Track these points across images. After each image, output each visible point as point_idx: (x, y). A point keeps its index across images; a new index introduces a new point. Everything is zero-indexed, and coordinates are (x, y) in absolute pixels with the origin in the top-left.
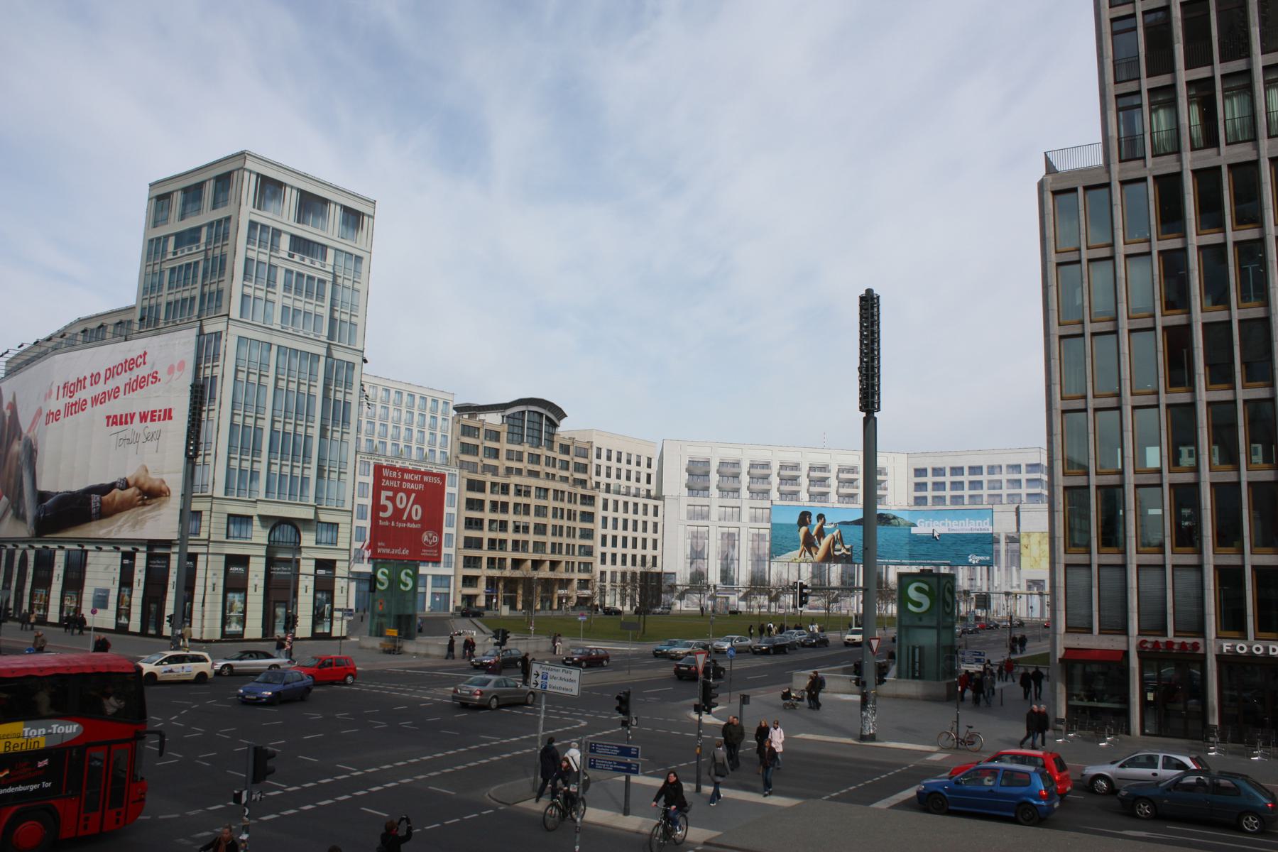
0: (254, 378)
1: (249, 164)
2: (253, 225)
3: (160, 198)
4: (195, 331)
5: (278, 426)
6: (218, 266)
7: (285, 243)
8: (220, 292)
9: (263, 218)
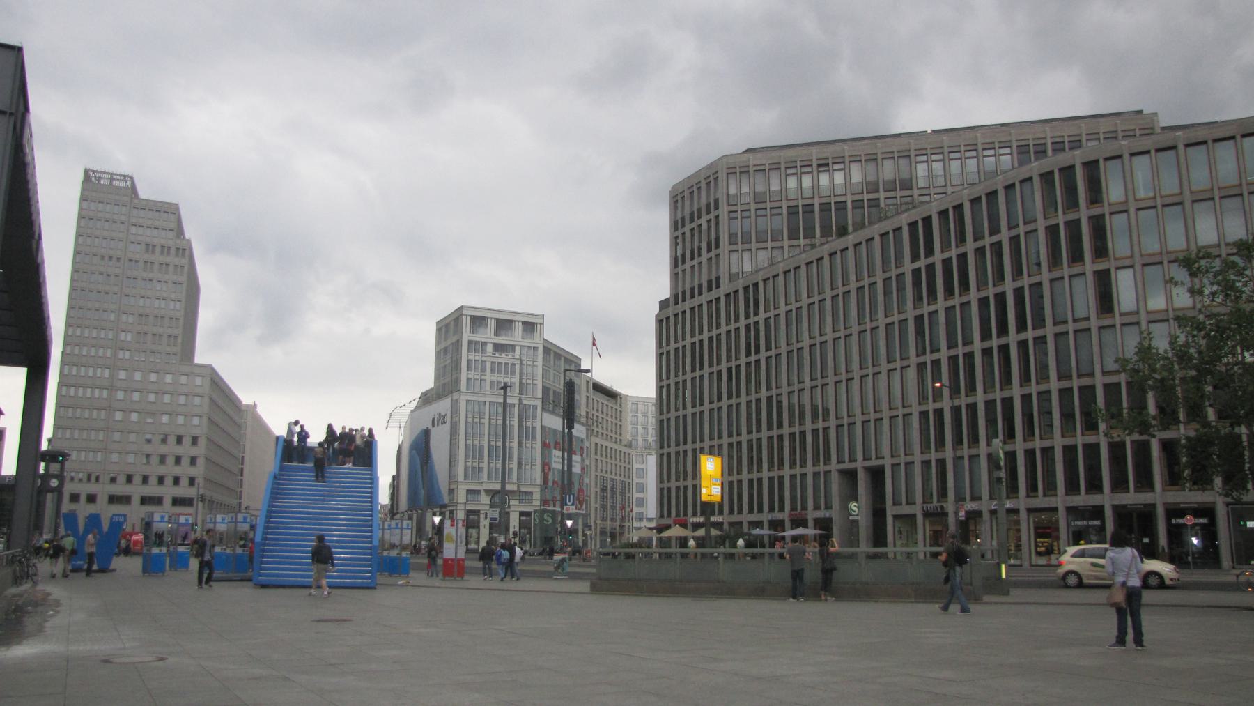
0: (477, 420)
5: (493, 443)
7: (489, 348)
9: (474, 338)
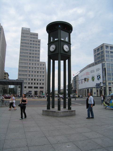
1: (104, 45)
2: (106, 51)
3: (95, 51)
4: (101, 64)
6: (103, 56)
7: (110, 52)
8: (104, 59)
